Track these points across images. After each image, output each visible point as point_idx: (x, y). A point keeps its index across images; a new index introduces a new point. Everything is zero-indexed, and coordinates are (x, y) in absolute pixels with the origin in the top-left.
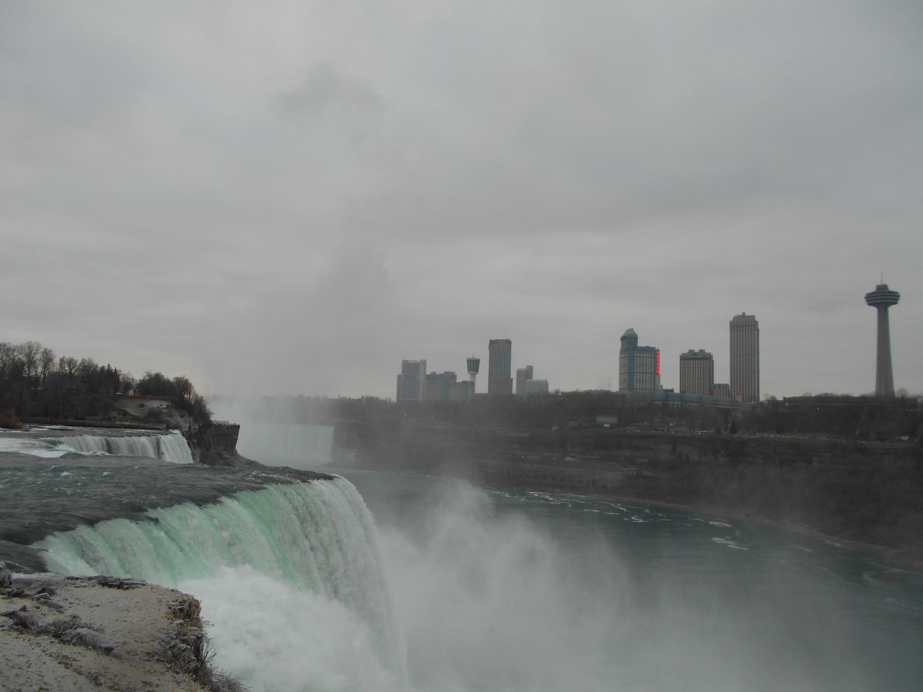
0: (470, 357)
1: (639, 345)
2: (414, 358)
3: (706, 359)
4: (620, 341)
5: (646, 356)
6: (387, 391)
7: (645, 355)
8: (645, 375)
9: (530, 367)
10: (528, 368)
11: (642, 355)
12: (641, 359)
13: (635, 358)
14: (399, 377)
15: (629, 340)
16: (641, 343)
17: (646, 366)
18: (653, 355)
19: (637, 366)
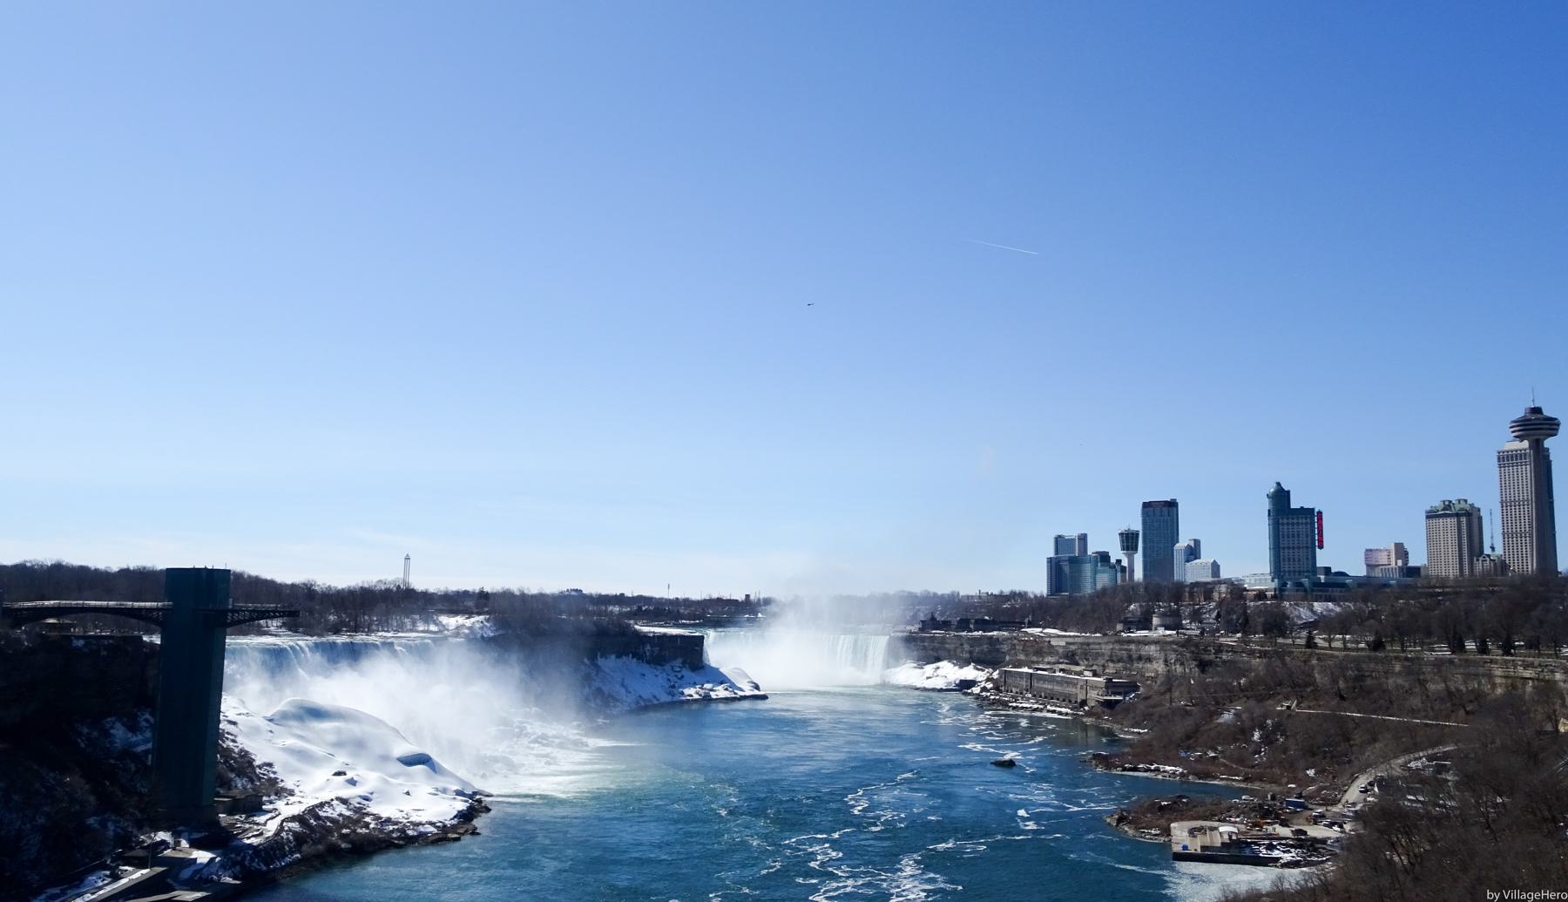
0: (1123, 528)
1: (1292, 507)
2: (1071, 532)
3: (1462, 515)
4: (1267, 501)
5: (1298, 523)
6: (1037, 585)
7: (1295, 521)
8: (1296, 550)
9: (1195, 540)
10: (1192, 544)
11: (1290, 521)
12: (1290, 526)
13: (1281, 527)
14: (1050, 560)
15: (1280, 497)
16: (1295, 504)
17: (1298, 535)
18: (1309, 520)
19: (1283, 537)
